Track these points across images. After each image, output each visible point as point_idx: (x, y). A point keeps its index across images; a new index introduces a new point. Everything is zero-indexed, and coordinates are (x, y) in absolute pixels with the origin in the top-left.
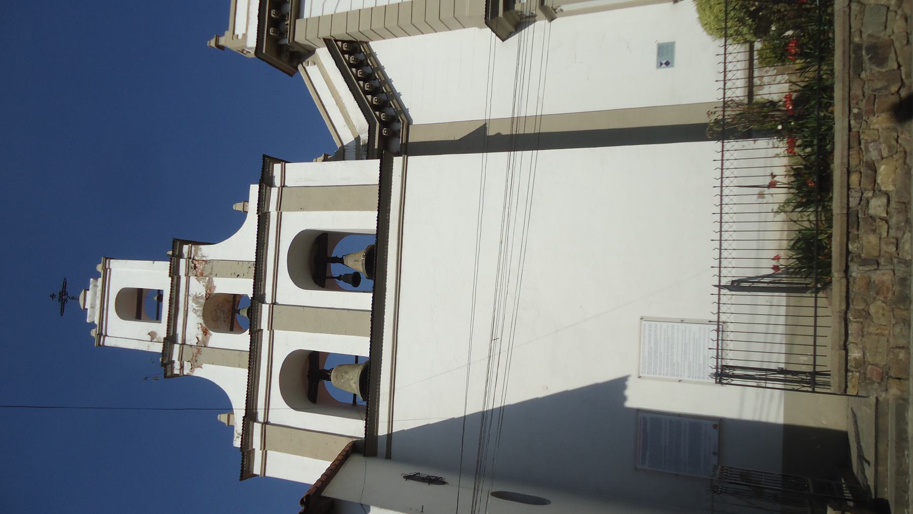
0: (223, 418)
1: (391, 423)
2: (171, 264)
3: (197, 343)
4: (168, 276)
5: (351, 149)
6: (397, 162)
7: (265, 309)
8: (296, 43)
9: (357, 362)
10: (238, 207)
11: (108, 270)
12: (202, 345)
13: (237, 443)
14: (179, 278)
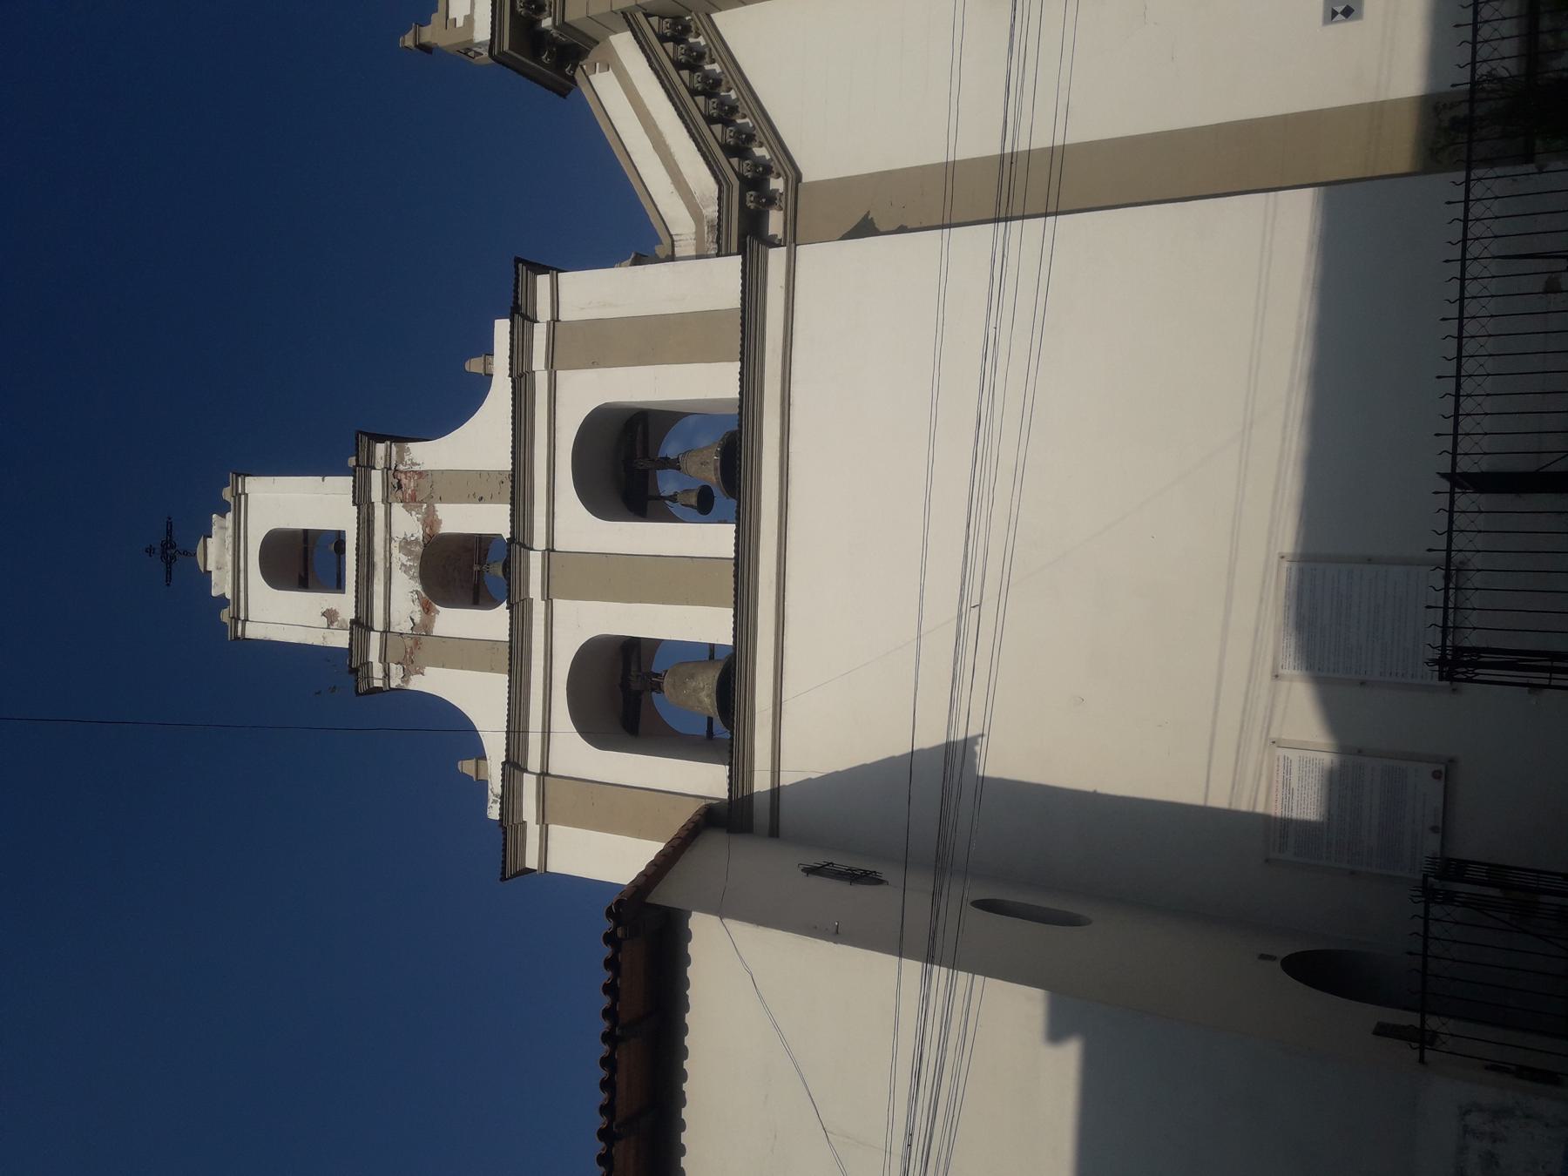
0: (467, 767)
1: (777, 774)
2: (354, 481)
3: (412, 628)
5: (687, 240)
6: (776, 259)
7: (535, 560)
9: (712, 657)
10: (474, 365)
11: (243, 497)
12: (422, 631)
13: (494, 812)
14: (371, 505)
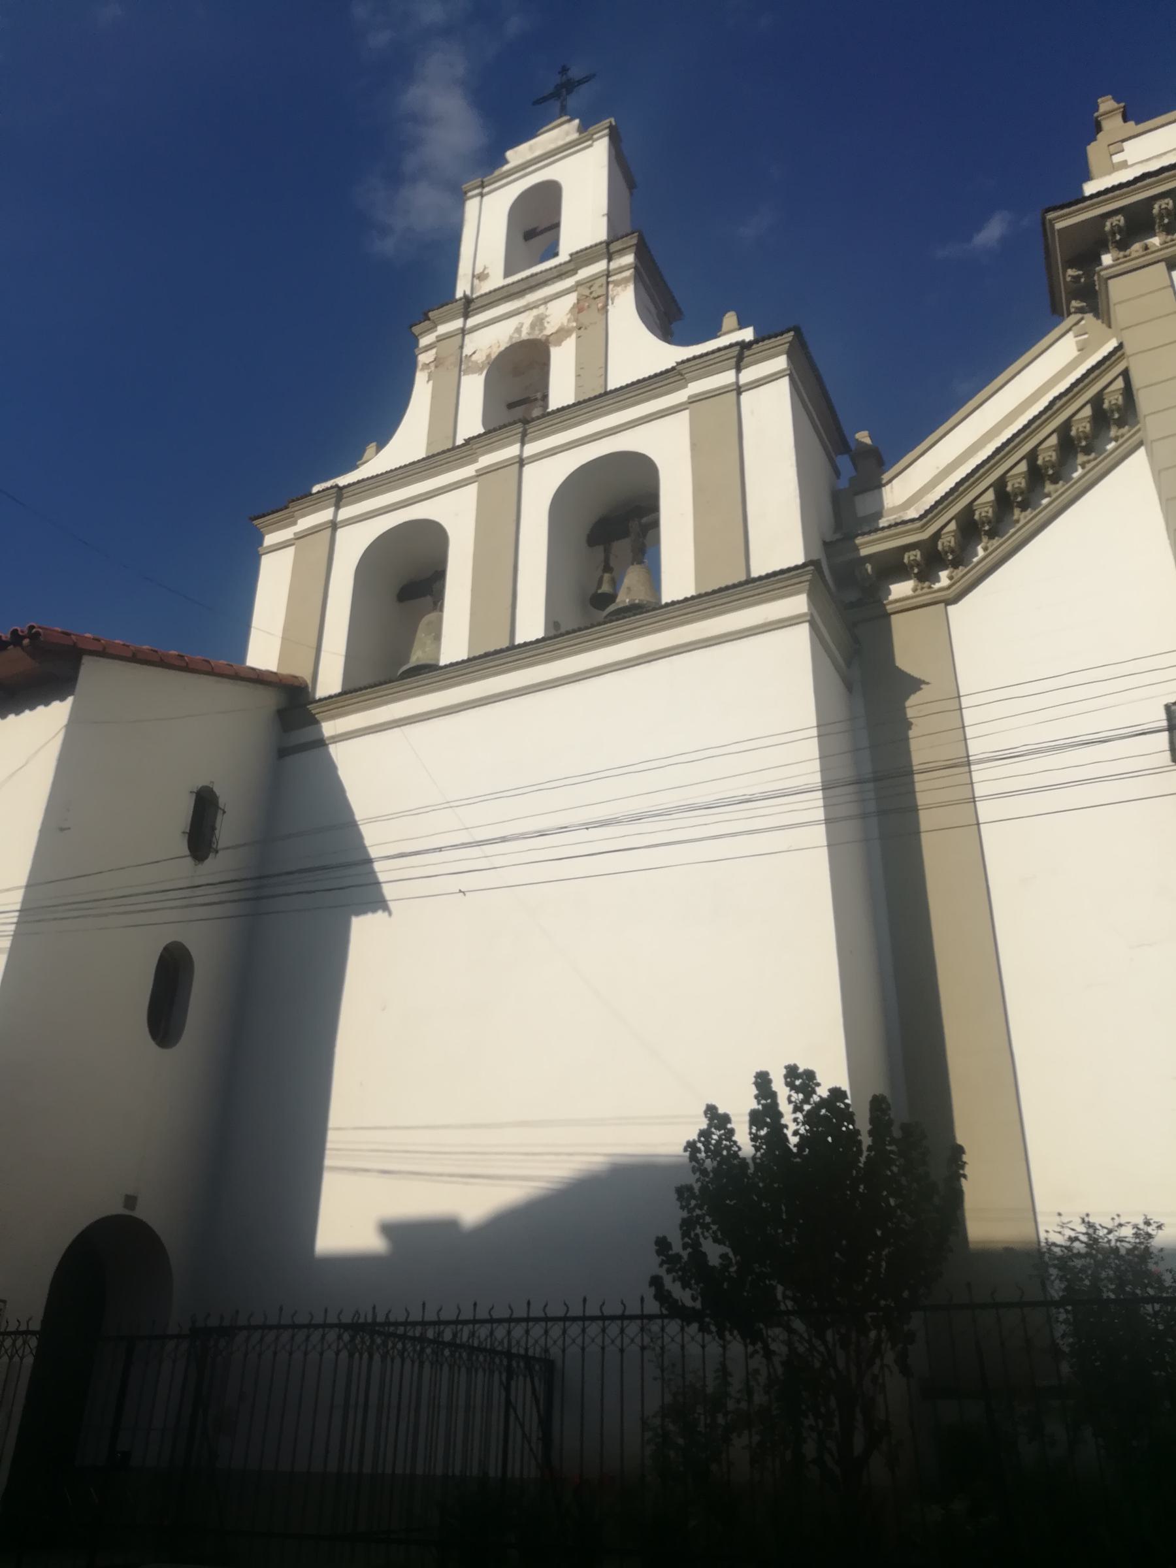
4: (570, 252)
8: (1106, 284)
11: (590, 142)
12: (462, 365)
14: (574, 272)
